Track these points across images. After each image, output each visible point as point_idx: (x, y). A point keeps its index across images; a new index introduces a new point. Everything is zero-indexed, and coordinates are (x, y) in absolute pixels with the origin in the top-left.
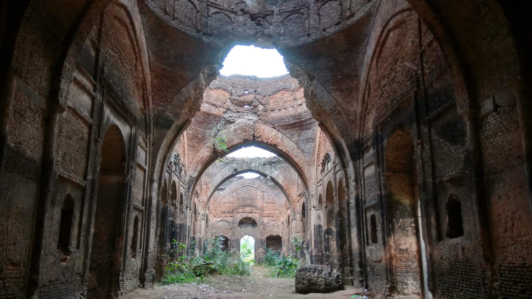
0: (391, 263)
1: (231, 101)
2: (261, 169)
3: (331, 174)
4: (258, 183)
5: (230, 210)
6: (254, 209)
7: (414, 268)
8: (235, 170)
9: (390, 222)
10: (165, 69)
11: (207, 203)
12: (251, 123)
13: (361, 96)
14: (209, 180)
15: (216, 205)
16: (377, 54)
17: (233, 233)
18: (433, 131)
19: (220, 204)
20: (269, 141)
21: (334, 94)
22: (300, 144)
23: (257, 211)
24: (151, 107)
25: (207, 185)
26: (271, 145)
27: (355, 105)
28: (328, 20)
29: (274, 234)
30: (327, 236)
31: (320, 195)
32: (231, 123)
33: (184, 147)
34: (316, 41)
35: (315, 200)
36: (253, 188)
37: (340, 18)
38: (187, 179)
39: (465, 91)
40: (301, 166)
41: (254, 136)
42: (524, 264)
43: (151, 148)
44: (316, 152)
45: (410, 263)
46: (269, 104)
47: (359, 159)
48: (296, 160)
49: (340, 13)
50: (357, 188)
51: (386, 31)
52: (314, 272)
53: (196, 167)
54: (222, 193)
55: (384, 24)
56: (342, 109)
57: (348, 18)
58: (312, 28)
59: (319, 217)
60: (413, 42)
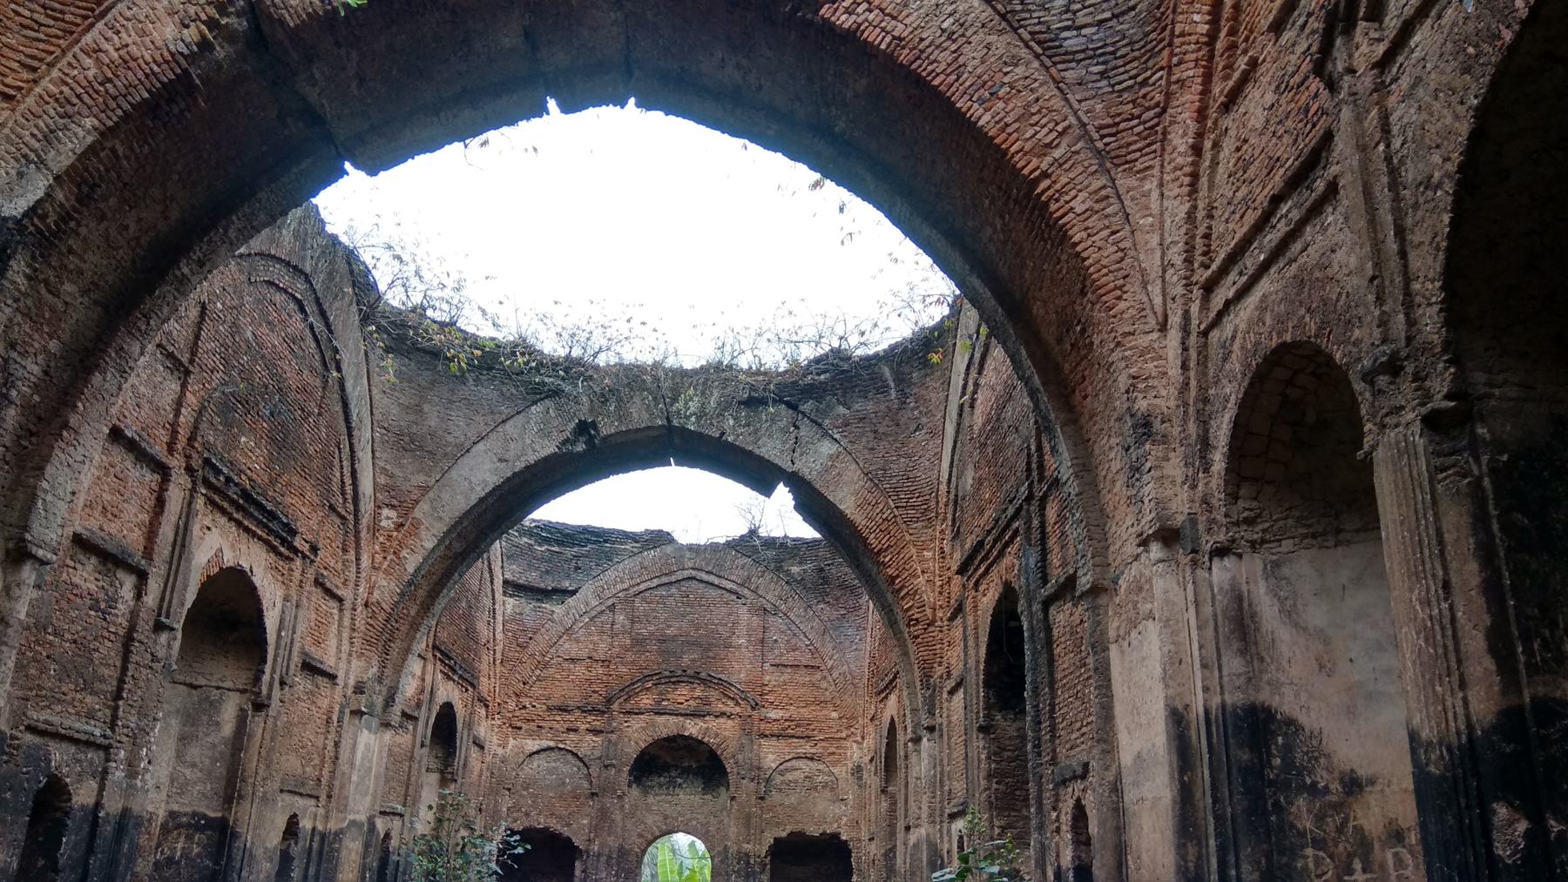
2: (733, 429)
4: (740, 567)
5: (595, 698)
6: (713, 694)
8: (583, 428)
14: (420, 479)
15: (526, 670)
17: (603, 815)
19: (546, 666)
23: (730, 707)
25: (405, 507)
29: (813, 830)
35: (1175, 468)
36: (713, 592)
40: (1030, 166)
53: (49, 137)
54: (559, 610)
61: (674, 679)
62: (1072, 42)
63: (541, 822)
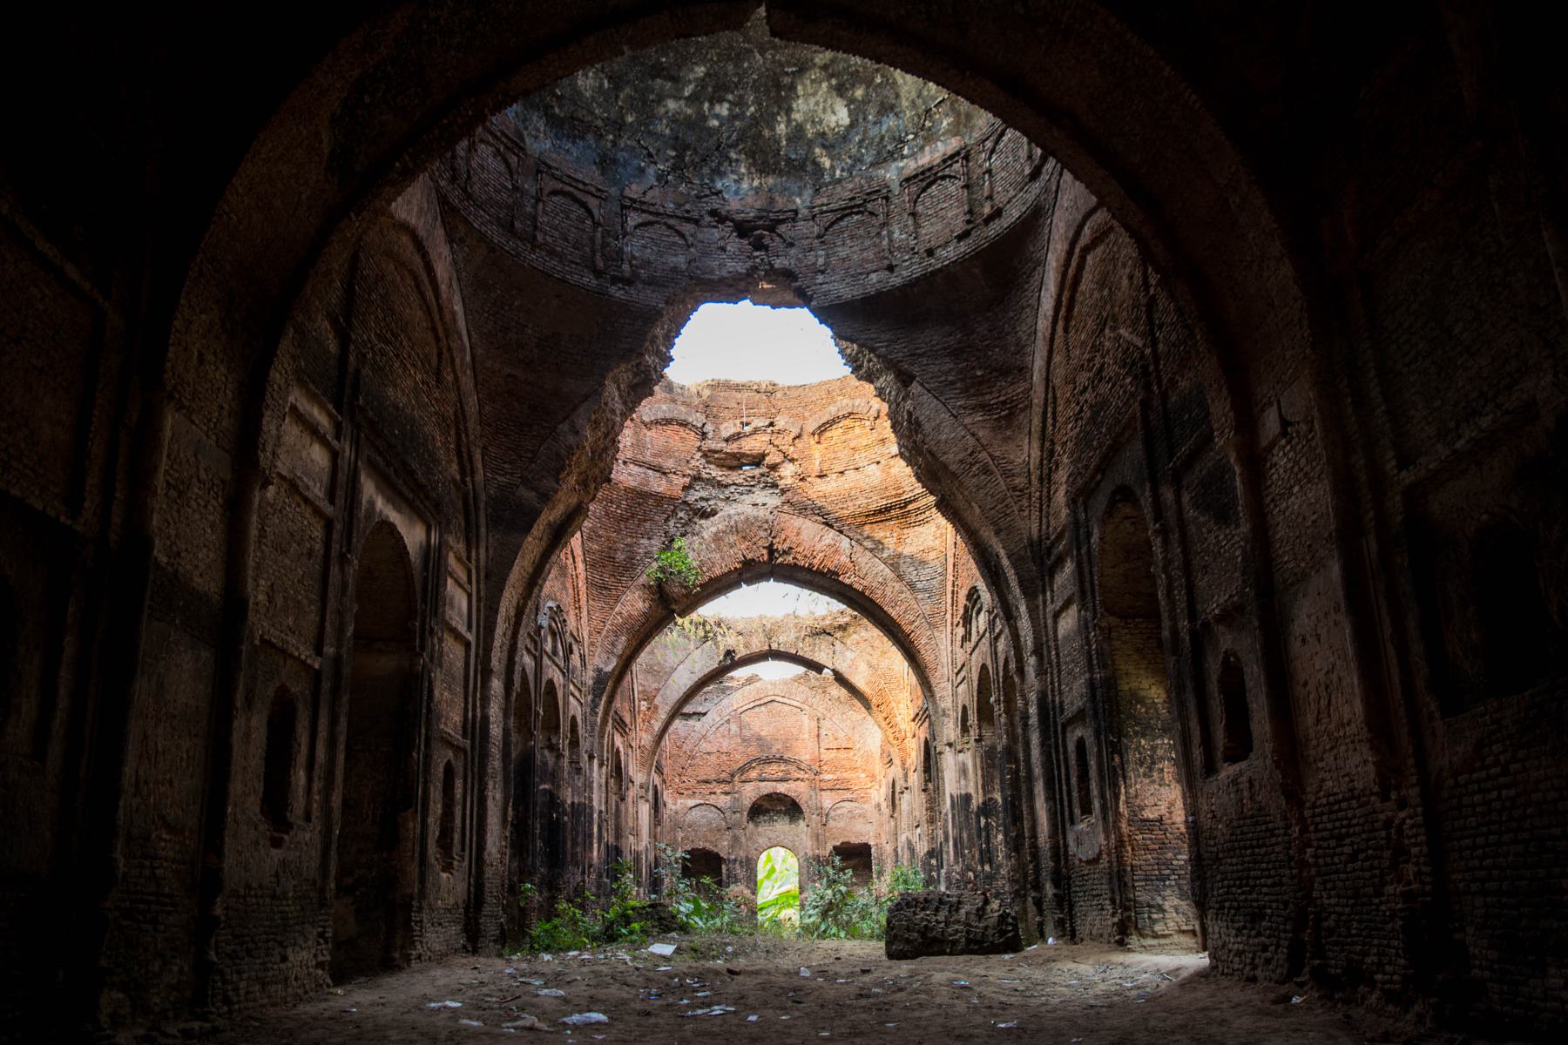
0: (1120, 858)
1: (705, 455)
3: (985, 645)
5: (723, 775)
6: (792, 768)
7: (1181, 867)
9: (1117, 749)
10: (514, 377)
11: (654, 753)
12: (762, 513)
13: (1036, 421)
14: (656, 685)
15: (682, 761)
16: (1063, 312)
17: (736, 839)
18: (1186, 498)
20: (816, 561)
21: (967, 421)
22: (903, 568)
23: (801, 775)
24: (480, 476)
26: (819, 573)
27: (1026, 448)
28: (939, 227)
29: (855, 840)
30: (983, 821)
31: (964, 708)
32: (706, 515)
33: (575, 588)
34: (912, 284)
35: (951, 725)
36: (786, 708)
37: (968, 222)
38: (589, 677)
39: (1225, 392)
40: (907, 629)
41: (771, 550)
42: (1351, 790)
43: (482, 586)
44: (949, 588)
45: (1170, 855)
46: (810, 457)
47: (1044, 592)
48: (893, 613)
49: (966, 208)
50: (1041, 672)
51: (1077, 250)
52: (937, 910)
54: (698, 725)
55: (1071, 234)
56: (993, 458)
57: (989, 220)
58: (899, 248)
59: (963, 771)
60: (1131, 277)
61: (768, 761)
62: (919, 586)
63: (701, 845)
